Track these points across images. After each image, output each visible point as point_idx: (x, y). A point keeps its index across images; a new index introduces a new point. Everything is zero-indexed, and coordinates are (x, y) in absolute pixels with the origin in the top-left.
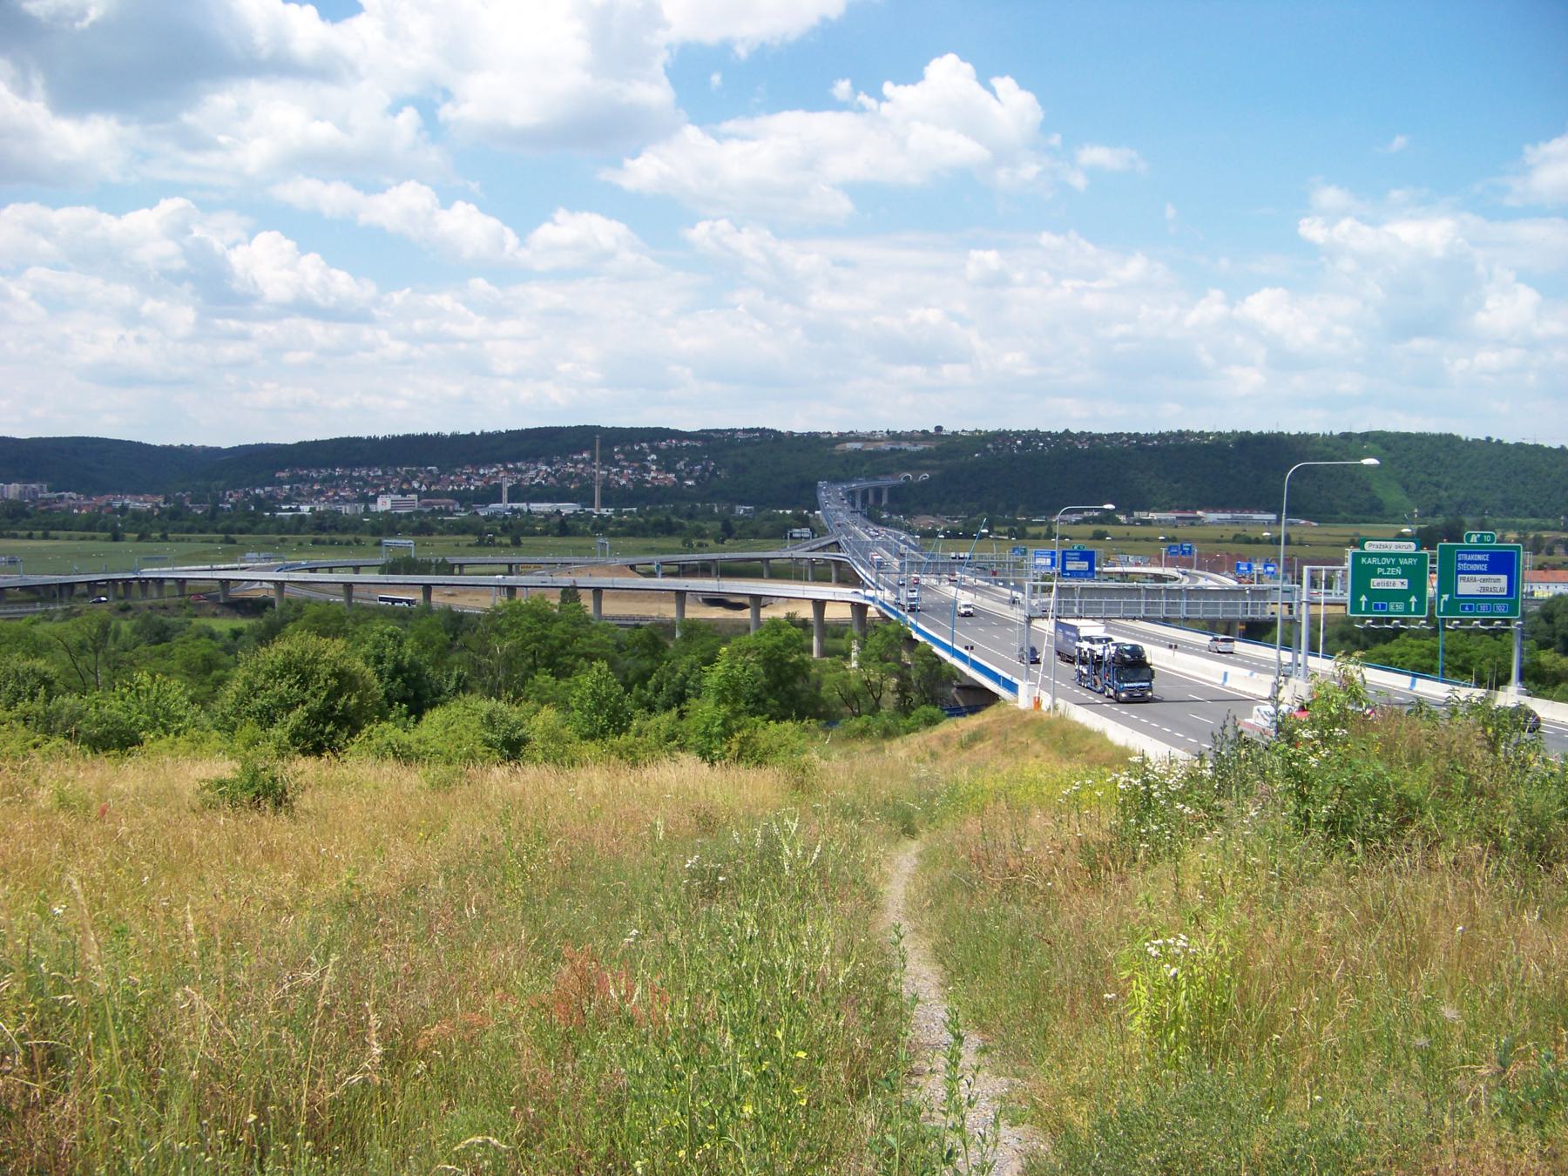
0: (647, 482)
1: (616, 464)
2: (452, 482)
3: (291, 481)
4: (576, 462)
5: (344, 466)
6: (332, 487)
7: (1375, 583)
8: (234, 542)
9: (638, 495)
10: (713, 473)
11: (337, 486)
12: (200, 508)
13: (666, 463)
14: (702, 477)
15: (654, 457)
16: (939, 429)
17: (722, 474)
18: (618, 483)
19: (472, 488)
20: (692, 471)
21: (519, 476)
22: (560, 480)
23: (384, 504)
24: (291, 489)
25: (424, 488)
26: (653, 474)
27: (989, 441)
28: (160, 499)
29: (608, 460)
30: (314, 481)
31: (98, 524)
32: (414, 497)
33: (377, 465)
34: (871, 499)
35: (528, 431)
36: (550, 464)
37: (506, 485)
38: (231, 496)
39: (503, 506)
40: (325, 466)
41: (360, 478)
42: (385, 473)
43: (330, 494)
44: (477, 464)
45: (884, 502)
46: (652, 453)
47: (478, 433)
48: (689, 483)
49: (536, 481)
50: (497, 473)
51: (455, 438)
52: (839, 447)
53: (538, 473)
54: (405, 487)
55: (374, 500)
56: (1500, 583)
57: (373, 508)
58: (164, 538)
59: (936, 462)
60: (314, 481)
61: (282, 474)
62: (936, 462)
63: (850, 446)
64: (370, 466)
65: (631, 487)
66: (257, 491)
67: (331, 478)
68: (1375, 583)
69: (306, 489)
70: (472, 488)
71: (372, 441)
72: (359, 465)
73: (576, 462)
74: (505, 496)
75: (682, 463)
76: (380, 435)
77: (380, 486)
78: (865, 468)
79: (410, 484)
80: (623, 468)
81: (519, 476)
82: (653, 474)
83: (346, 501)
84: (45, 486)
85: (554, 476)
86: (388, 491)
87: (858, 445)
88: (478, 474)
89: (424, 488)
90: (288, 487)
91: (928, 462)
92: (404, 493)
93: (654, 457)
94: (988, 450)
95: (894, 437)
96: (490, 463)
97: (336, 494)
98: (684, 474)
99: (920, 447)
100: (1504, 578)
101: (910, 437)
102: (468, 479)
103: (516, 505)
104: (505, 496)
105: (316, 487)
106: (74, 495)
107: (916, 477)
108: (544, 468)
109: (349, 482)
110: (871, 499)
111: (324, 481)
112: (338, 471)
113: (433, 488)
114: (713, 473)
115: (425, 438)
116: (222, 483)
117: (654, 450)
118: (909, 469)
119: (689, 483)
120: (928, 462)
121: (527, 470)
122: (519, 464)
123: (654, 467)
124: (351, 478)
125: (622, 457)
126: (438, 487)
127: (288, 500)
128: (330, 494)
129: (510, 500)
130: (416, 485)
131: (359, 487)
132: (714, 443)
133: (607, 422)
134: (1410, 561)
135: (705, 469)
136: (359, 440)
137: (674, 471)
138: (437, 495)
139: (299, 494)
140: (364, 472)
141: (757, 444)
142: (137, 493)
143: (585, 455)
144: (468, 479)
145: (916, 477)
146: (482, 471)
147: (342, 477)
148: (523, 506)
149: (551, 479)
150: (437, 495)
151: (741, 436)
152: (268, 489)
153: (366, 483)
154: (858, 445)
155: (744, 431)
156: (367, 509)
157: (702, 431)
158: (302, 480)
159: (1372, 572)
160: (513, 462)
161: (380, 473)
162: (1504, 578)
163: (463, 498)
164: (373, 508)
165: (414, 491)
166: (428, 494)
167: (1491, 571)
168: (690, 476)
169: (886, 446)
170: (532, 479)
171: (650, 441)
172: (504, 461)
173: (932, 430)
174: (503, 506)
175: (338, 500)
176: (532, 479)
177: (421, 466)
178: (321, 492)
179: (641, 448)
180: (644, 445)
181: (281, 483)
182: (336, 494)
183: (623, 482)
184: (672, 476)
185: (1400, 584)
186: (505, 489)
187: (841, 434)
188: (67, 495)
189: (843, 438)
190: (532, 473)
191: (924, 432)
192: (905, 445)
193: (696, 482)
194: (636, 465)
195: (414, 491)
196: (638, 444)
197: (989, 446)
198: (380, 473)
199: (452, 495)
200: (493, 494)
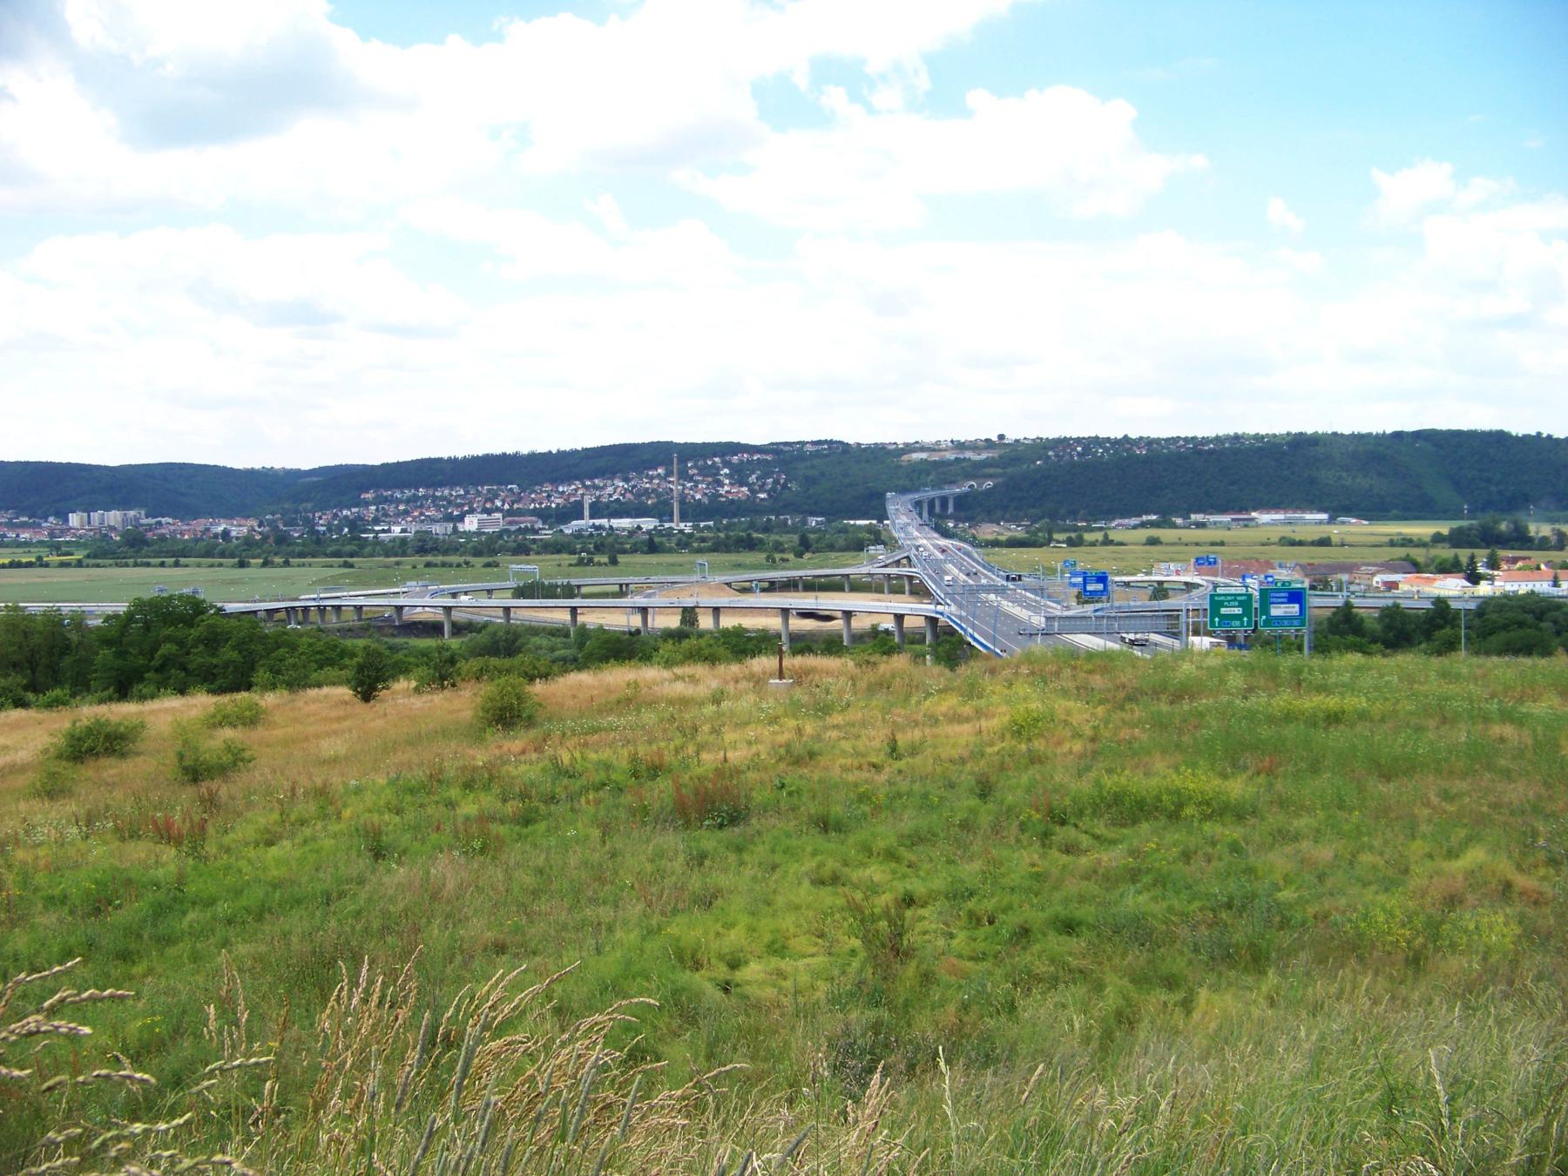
0: (721, 495)
1: (691, 479)
2: (533, 501)
3: (376, 501)
4: (652, 478)
5: (427, 486)
6: (416, 507)
7: (1223, 611)
8: (352, 566)
9: (714, 509)
10: (784, 486)
11: (422, 506)
12: (295, 531)
13: (739, 477)
14: (773, 489)
15: (726, 471)
16: (1001, 437)
17: (793, 486)
18: (693, 497)
19: (553, 505)
20: (764, 484)
21: (598, 493)
22: (638, 495)
23: (471, 524)
24: (377, 510)
25: (506, 507)
26: (726, 488)
27: (1052, 449)
28: (255, 523)
29: (684, 476)
30: (399, 502)
31: (216, 551)
32: (498, 515)
33: (459, 484)
34: (937, 509)
35: (603, 448)
36: (626, 480)
37: (588, 500)
38: (320, 518)
39: (585, 523)
40: (409, 486)
41: (443, 498)
42: (467, 492)
43: (416, 514)
44: (556, 481)
45: (950, 510)
46: (725, 467)
47: (554, 452)
48: (762, 496)
49: (615, 497)
50: (576, 490)
51: (533, 457)
52: (905, 457)
53: (615, 489)
54: (488, 506)
55: (461, 518)
56: (1294, 609)
57: (461, 527)
58: (287, 564)
59: (999, 471)
60: (399, 502)
61: (367, 496)
62: (999, 471)
63: (916, 456)
64: (452, 485)
65: (706, 501)
66: (345, 512)
67: (415, 498)
68: (1223, 611)
69: (391, 509)
70: (553, 505)
71: (453, 462)
72: (442, 485)
73: (652, 478)
74: (587, 513)
75: (754, 476)
76: (460, 455)
77: (463, 505)
78: (931, 478)
79: (493, 503)
80: (697, 482)
81: (598, 493)
82: (726, 488)
83: (433, 520)
84: (143, 512)
85: (631, 492)
86: (472, 511)
87: (924, 455)
88: (557, 491)
89: (506, 507)
90: (373, 508)
91: (991, 471)
92: (489, 512)
93: (726, 471)
94: (1049, 457)
95: (960, 446)
96: (568, 480)
97: (422, 514)
98: (757, 488)
99: (984, 456)
100: (1297, 606)
101: (973, 446)
102: (549, 496)
103: (597, 522)
104: (587, 513)
105: (402, 507)
106: (170, 520)
107: (980, 485)
108: (621, 484)
109: (433, 502)
110: (937, 509)
111: (408, 502)
112: (422, 491)
113: (516, 506)
114: (784, 486)
115: (504, 457)
116: (309, 505)
117: (727, 464)
118: (973, 477)
119: (762, 496)
120: (991, 471)
121: (605, 487)
122: (596, 481)
123: (727, 481)
124: (435, 498)
125: (696, 471)
126: (520, 506)
127: (376, 521)
128: (416, 514)
129: (592, 517)
130: (498, 503)
131: (443, 506)
132: (784, 456)
133: (680, 438)
134: (1243, 598)
135: (776, 482)
136: (440, 460)
137: (747, 484)
138: (520, 513)
139: (386, 515)
140: (446, 492)
141: (826, 456)
142: (229, 516)
143: (660, 471)
144: (549, 496)
145: (980, 485)
146: (561, 489)
147: (425, 497)
148: (604, 522)
149: (629, 495)
150: (520, 513)
151: (809, 448)
152: (354, 510)
153: (450, 502)
154: (924, 455)
155: (813, 443)
156: (455, 528)
157: (772, 444)
158: (386, 500)
159: (1221, 604)
160: (591, 478)
161: (462, 492)
162: (1297, 606)
163: (543, 515)
164: (461, 527)
165: (498, 510)
166: (510, 513)
167: (1289, 602)
168: (762, 489)
169: (950, 456)
170: (610, 496)
171: (722, 456)
172: (580, 478)
173: (995, 438)
174: (585, 523)
175: (422, 521)
176: (610, 496)
177: (501, 484)
178: (406, 513)
179: (714, 463)
180: (717, 459)
181: (367, 504)
182: (422, 514)
183: (698, 496)
184: (745, 489)
185: (1238, 611)
186: (586, 506)
187: (907, 445)
188: (163, 520)
189: (909, 448)
190: (610, 490)
191: (987, 440)
192: (969, 455)
193: (769, 495)
194: (710, 479)
195: (498, 510)
196: (711, 459)
197: (1051, 453)
198: (462, 492)
199: (535, 512)
200: (575, 511)
